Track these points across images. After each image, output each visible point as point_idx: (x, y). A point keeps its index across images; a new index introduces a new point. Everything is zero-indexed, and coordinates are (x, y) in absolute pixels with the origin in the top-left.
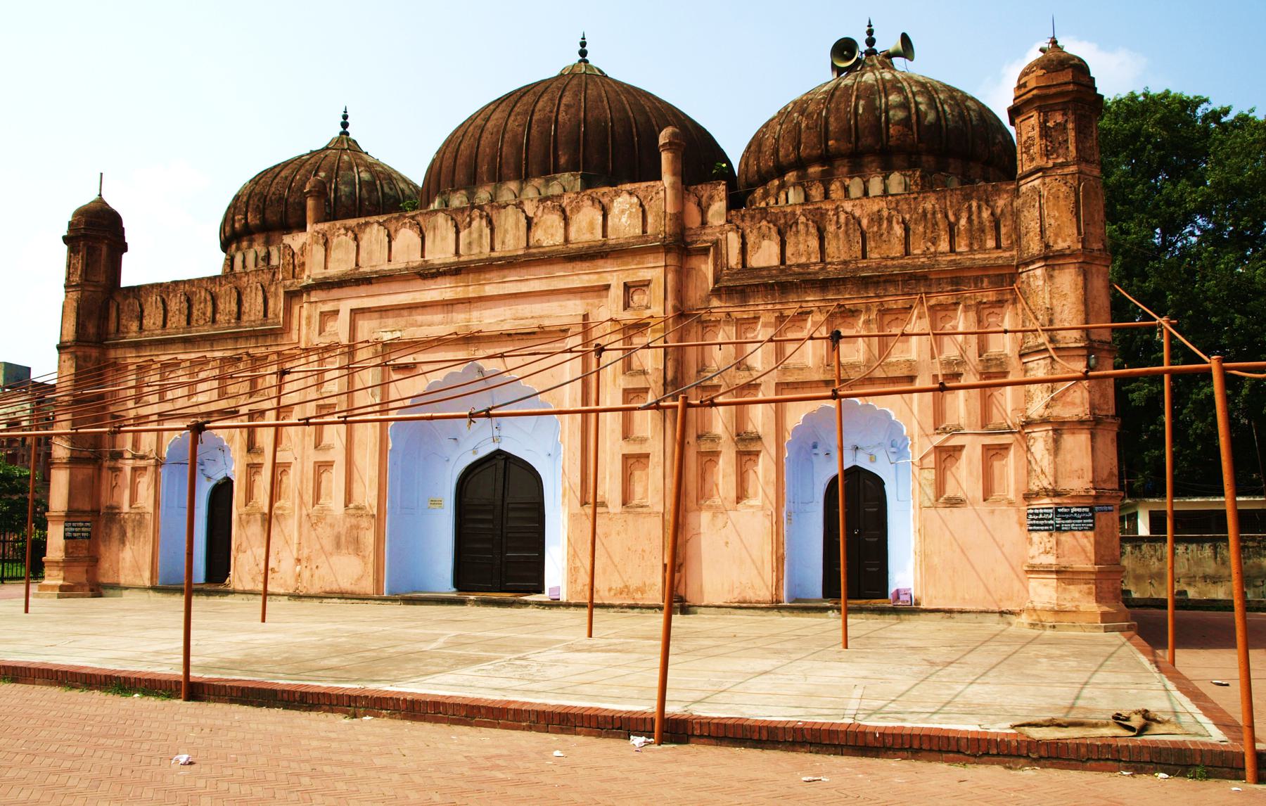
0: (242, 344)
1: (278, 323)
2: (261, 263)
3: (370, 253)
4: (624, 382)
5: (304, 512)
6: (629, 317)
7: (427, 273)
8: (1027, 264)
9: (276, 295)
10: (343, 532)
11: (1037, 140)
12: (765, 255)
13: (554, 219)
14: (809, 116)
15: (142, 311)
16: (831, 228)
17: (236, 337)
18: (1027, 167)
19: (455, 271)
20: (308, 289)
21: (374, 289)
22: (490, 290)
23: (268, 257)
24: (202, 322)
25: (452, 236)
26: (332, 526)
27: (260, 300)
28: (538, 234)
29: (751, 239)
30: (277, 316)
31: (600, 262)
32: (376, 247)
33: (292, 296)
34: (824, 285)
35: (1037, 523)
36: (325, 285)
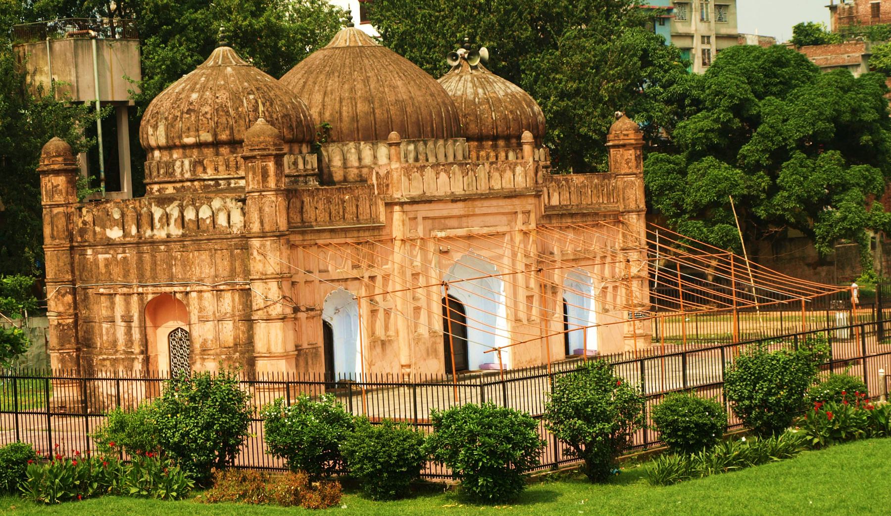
0: (362, 234)
1: (380, 222)
2: (293, 167)
3: (429, 184)
4: (524, 260)
5: (411, 336)
6: (524, 228)
7: (455, 200)
8: (629, 212)
9: (376, 204)
10: (430, 346)
11: (633, 160)
12: (555, 201)
13: (496, 175)
14: (511, 112)
15: (302, 208)
16: (573, 189)
17: (359, 230)
18: (627, 171)
19: (466, 199)
20: (402, 204)
21: (432, 206)
22: (477, 211)
23: (295, 163)
24: (338, 218)
25: (461, 178)
26: (424, 343)
27: (368, 206)
28: (493, 183)
29: (551, 191)
30: (377, 217)
31: (514, 200)
32: (431, 182)
33: (389, 205)
34: (572, 215)
35: (634, 317)
36: (413, 202)
